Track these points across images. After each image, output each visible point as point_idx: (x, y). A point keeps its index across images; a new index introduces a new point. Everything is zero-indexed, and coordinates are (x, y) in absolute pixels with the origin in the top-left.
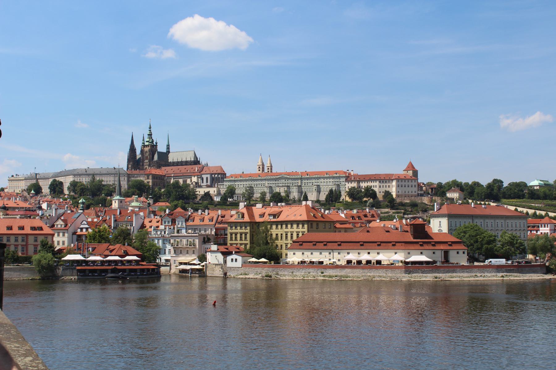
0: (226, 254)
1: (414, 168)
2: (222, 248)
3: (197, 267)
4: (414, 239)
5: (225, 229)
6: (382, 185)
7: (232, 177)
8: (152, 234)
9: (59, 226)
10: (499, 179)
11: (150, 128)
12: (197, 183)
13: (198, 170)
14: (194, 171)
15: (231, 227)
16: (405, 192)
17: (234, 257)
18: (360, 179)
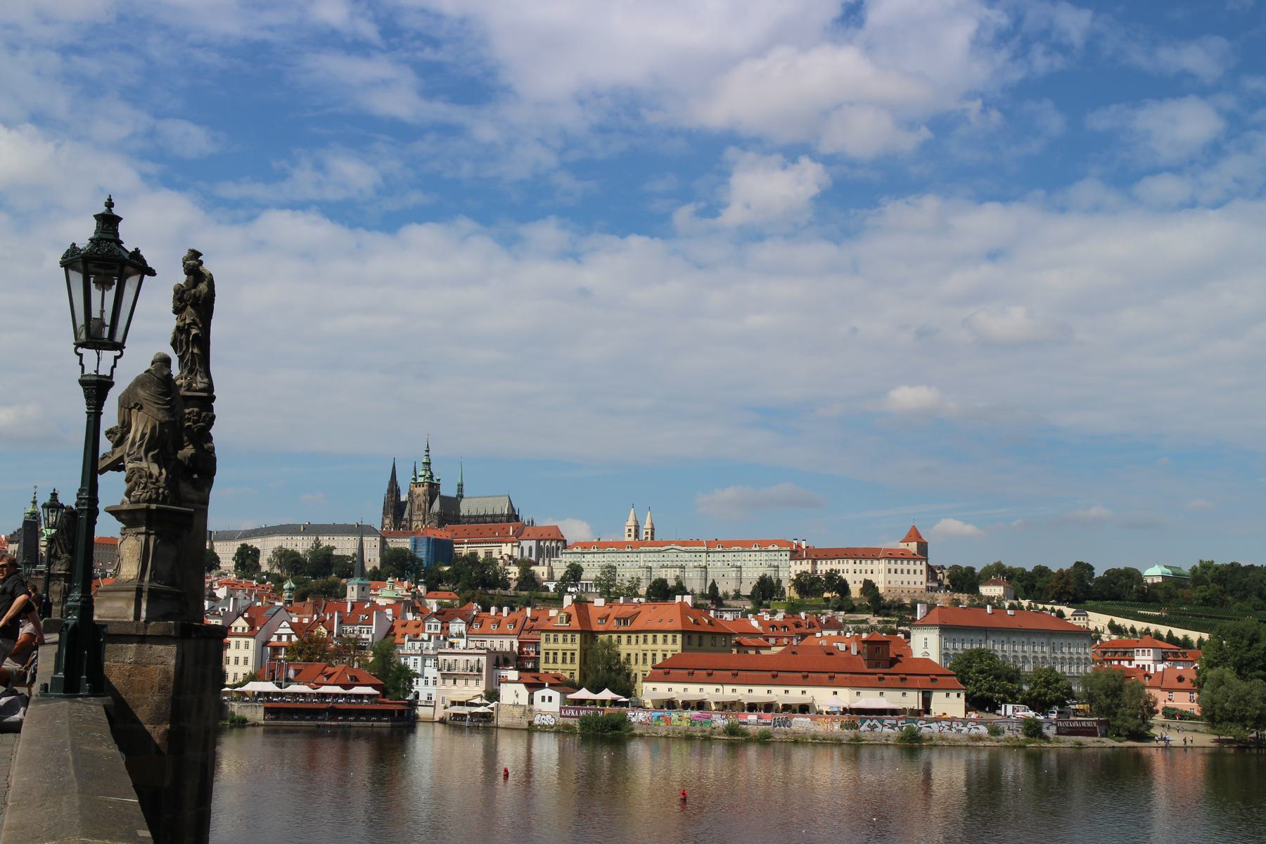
0: (533, 687)
1: (920, 537)
2: (529, 678)
3: (480, 710)
4: (869, 667)
5: (537, 644)
6: (858, 566)
7: (577, 548)
8: (406, 648)
9: (240, 630)
10: (1085, 562)
11: (428, 451)
12: (510, 557)
13: (514, 532)
14: (506, 535)
15: (547, 640)
16: (902, 583)
17: (547, 692)
18: (816, 555)
